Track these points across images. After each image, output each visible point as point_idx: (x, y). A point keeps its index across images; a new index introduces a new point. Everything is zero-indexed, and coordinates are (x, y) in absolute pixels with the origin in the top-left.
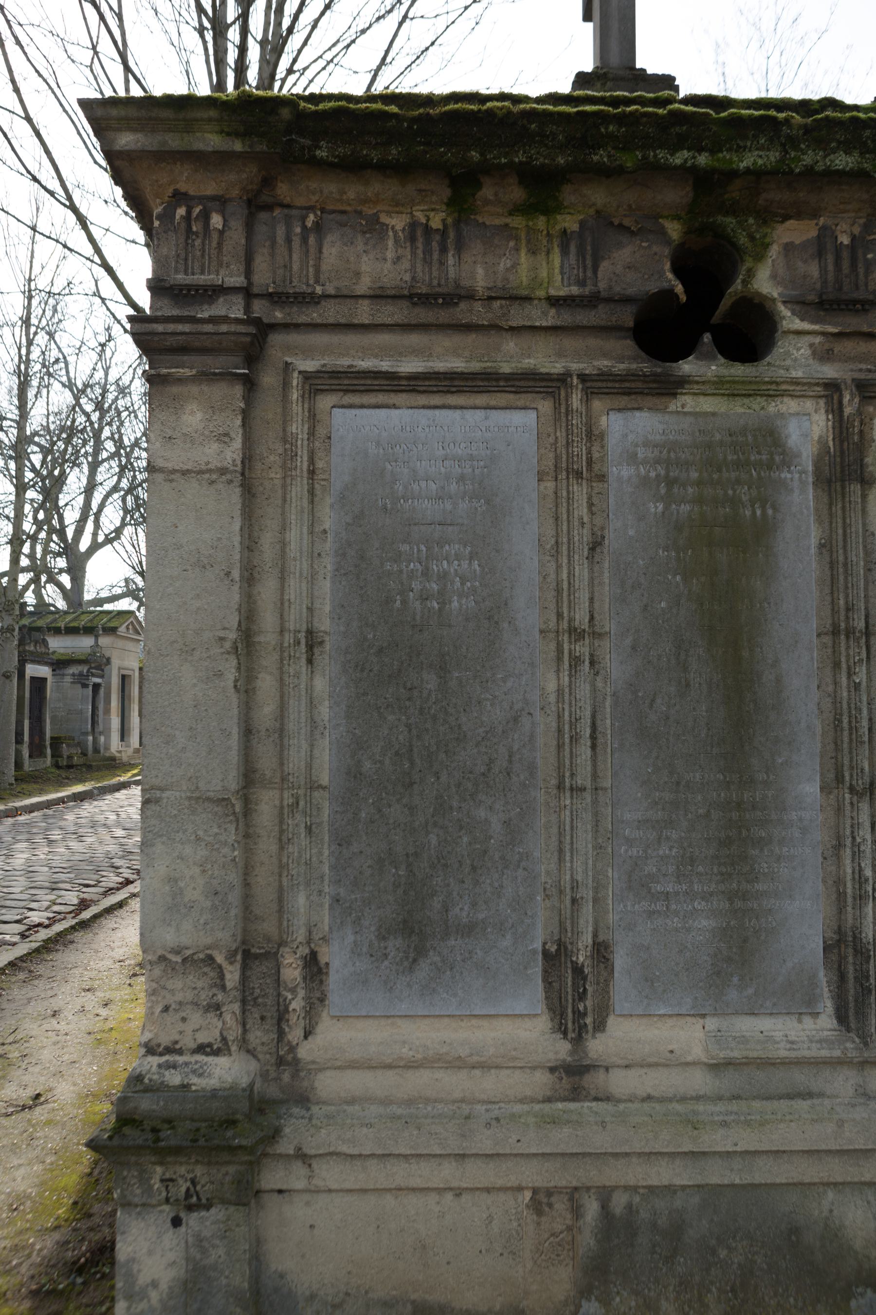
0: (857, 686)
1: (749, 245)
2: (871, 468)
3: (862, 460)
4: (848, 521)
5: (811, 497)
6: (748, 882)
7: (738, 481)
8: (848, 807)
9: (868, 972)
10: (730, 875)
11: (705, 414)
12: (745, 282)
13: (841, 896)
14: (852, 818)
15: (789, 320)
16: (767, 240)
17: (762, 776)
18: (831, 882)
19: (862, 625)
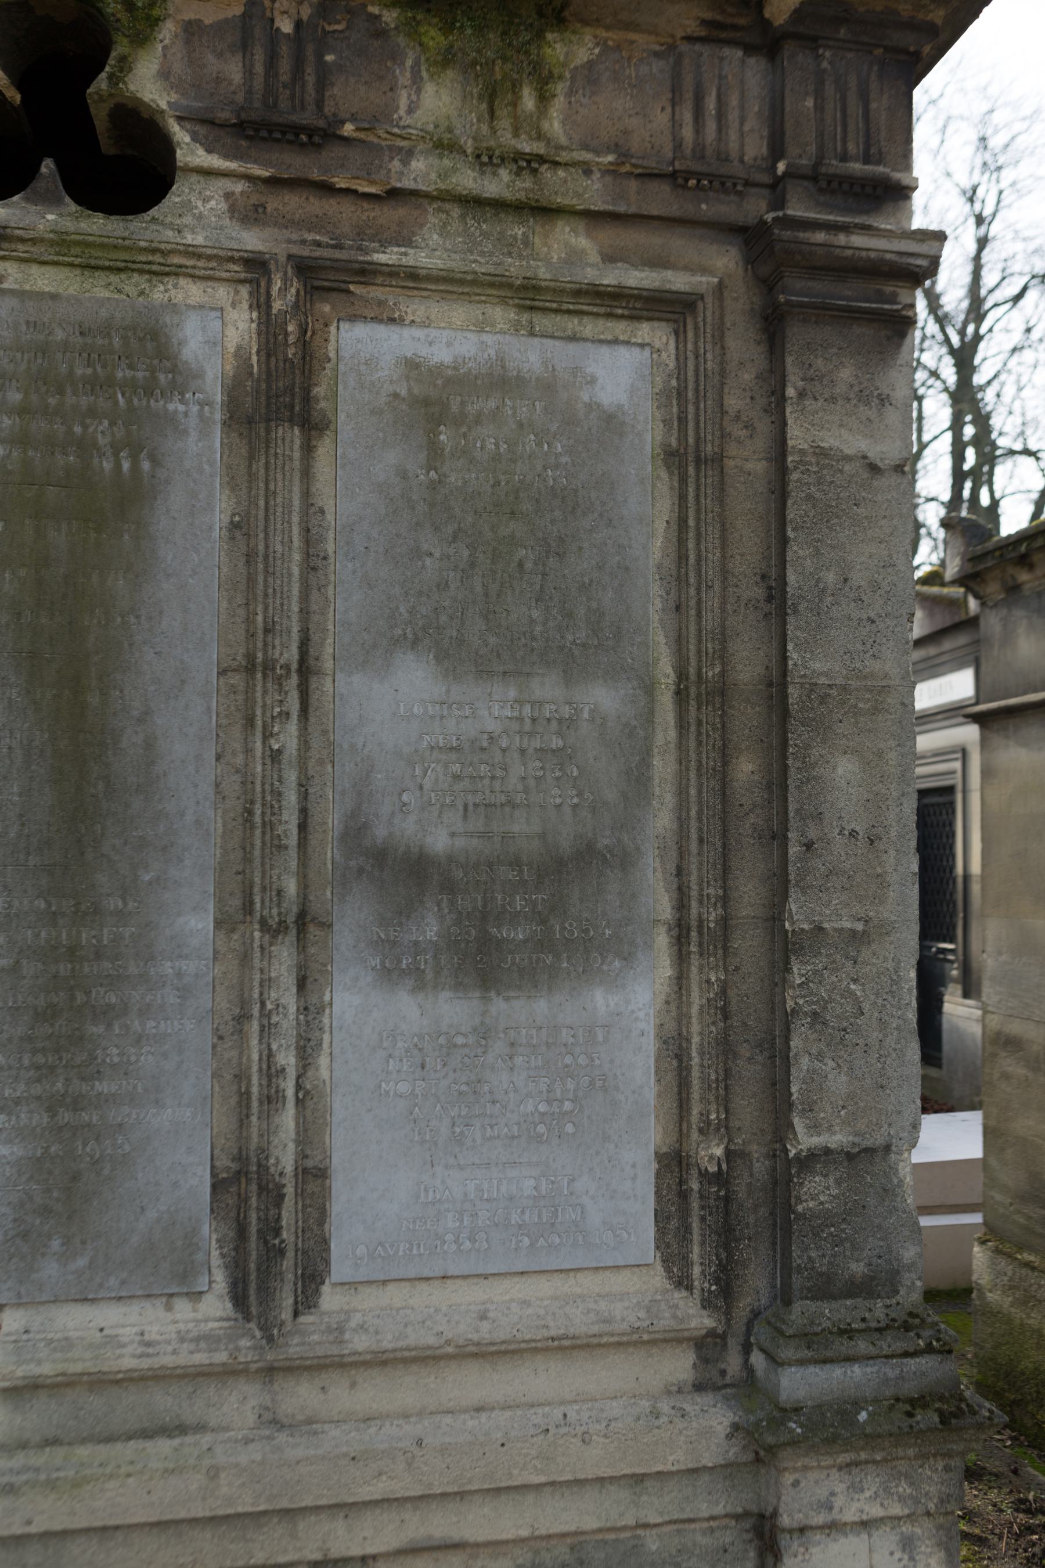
0: (275, 756)
1: (123, 16)
2: (323, 404)
3: (307, 391)
4: (272, 487)
5: (218, 445)
6: (83, 1079)
7: (92, 412)
8: (257, 954)
9: (279, 1219)
10: (52, 1069)
11: (40, 295)
12: (114, 79)
13: (244, 1097)
14: (262, 971)
15: (190, 152)
16: (156, 12)
17: (114, 903)
18: (229, 1077)
19: (292, 655)
